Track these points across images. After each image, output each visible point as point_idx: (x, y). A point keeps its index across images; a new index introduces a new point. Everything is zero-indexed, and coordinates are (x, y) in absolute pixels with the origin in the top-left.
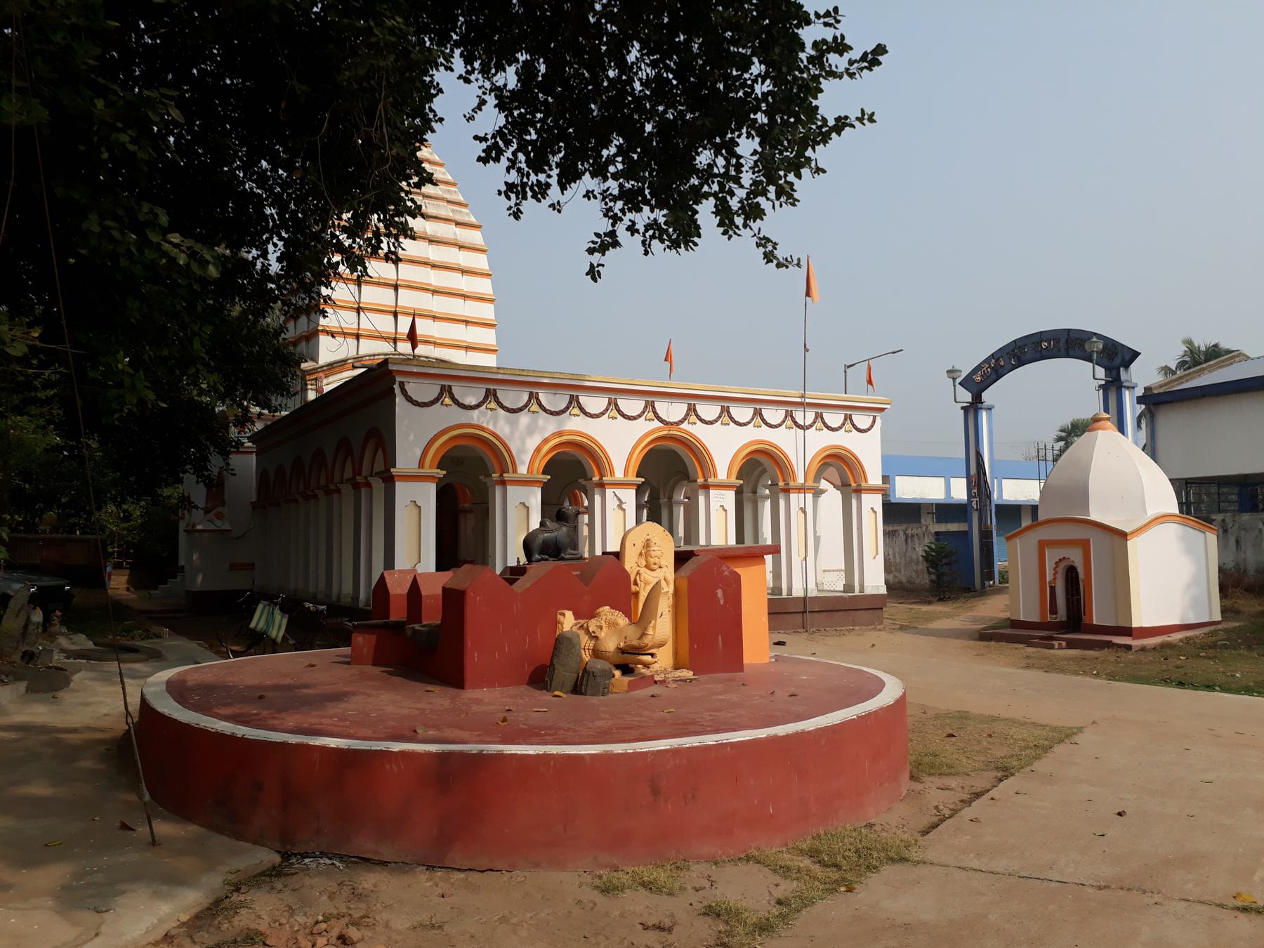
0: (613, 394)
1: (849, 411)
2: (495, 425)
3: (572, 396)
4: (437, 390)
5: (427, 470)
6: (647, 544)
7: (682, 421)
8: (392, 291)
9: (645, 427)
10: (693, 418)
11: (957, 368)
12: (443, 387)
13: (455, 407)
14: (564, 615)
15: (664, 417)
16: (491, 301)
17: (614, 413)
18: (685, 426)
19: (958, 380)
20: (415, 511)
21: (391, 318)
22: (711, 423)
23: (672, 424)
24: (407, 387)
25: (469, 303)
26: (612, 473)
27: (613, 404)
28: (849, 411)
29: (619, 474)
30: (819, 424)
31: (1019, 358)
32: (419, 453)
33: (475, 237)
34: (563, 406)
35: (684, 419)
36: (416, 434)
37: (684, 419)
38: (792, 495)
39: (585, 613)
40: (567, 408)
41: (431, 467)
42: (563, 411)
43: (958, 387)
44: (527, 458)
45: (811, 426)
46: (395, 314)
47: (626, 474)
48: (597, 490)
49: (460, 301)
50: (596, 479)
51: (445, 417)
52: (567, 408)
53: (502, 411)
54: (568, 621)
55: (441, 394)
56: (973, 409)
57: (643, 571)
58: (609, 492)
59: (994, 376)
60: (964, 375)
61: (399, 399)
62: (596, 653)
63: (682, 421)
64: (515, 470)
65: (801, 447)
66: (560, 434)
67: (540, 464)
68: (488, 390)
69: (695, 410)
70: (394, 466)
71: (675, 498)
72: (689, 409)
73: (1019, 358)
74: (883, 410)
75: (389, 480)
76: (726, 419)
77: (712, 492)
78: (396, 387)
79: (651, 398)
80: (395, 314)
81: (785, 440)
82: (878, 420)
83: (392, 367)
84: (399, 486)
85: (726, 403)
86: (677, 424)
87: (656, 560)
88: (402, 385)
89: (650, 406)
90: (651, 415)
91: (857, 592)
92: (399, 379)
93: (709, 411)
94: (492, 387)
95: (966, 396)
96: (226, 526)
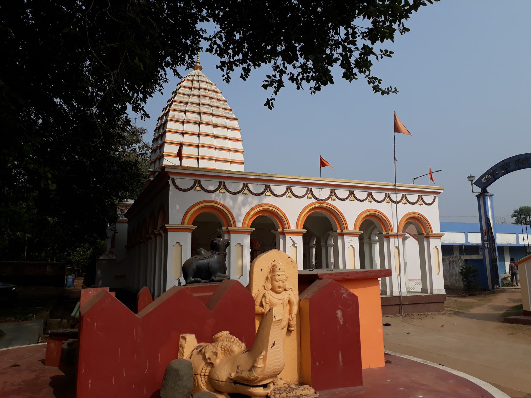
0: (289, 184)
1: (420, 193)
3: (266, 186)
4: (192, 183)
5: (186, 225)
6: (273, 270)
7: (327, 199)
8: (196, 149)
10: (334, 197)
11: (472, 175)
12: (196, 181)
13: (202, 191)
14: (185, 338)
15: (318, 197)
16: (242, 152)
17: (290, 195)
18: (329, 201)
19: (474, 182)
20: (180, 248)
21: (196, 161)
22: (344, 200)
23: (322, 200)
24: (176, 181)
25: (232, 153)
26: (289, 227)
27: (289, 190)
28: (420, 193)
29: (293, 228)
30: (404, 201)
31: (506, 169)
33: (235, 124)
34: (262, 190)
36: (180, 206)
38: (390, 239)
39: (206, 337)
40: (264, 192)
41: (188, 224)
42: (262, 194)
43: (474, 185)
44: (242, 219)
45: (400, 202)
46: (198, 159)
47: (297, 227)
48: (281, 236)
49: (228, 152)
50: (280, 230)
52: (264, 192)
53: (228, 194)
54: (190, 343)
55: (195, 184)
56: (482, 196)
57: (270, 294)
58: (287, 237)
59: (493, 179)
60: (476, 179)
61: (172, 187)
62: (211, 381)
63: (327, 199)
64: (235, 225)
65: (395, 213)
66: (260, 205)
67: (249, 222)
68: (220, 183)
69: (335, 193)
70: (168, 224)
71: (329, 242)
72: (331, 192)
73: (506, 169)
74: (439, 193)
75: (166, 231)
76: (352, 198)
77: (346, 238)
78: (170, 181)
79: (310, 186)
80: (198, 159)
81: (386, 209)
82: (437, 199)
83: (167, 170)
84: (170, 234)
85: (352, 189)
87: (281, 284)
88: (173, 180)
89: (309, 191)
90: (310, 196)
91: (429, 293)
92: (171, 176)
93: (343, 193)
94: (223, 181)
95: (478, 190)
96: (114, 257)
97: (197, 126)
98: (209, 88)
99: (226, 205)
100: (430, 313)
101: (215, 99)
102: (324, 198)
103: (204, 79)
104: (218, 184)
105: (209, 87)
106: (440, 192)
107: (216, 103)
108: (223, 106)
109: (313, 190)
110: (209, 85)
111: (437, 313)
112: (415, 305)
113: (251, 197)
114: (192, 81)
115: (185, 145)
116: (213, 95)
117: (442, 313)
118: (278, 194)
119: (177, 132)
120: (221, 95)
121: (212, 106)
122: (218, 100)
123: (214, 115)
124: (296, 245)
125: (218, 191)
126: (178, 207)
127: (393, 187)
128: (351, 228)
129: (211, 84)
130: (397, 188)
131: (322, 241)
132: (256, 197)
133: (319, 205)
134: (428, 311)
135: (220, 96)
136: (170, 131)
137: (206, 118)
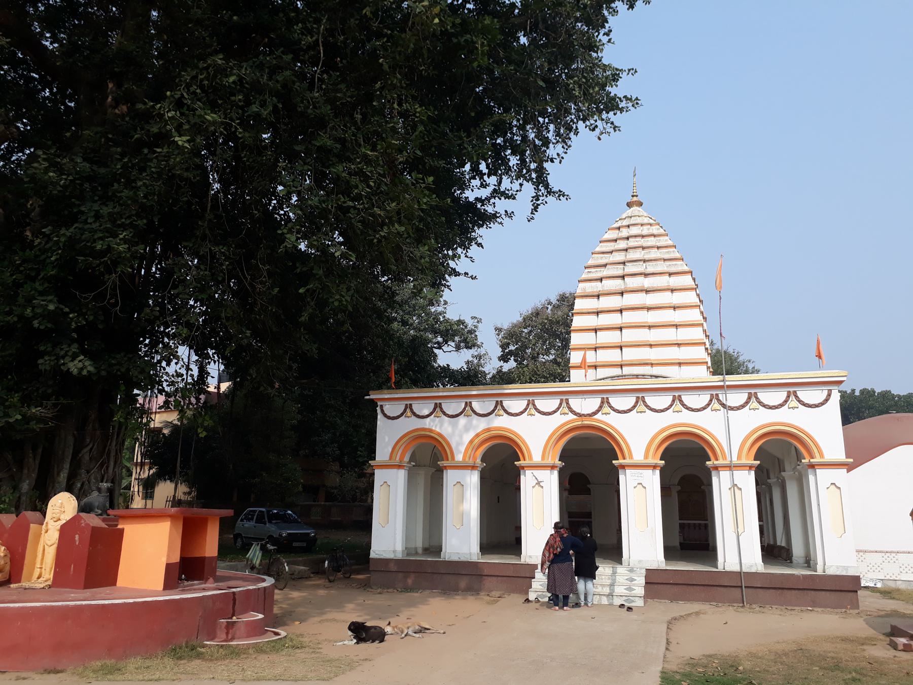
2: (441, 428)
4: (403, 407)
7: (595, 413)
10: (606, 409)
15: (578, 411)
17: (533, 411)
18: (599, 416)
24: (385, 409)
26: (531, 458)
28: (792, 388)
29: (537, 457)
32: (390, 450)
44: (463, 449)
46: (621, 348)
51: (409, 424)
52: (493, 411)
55: (405, 410)
61: (380, 416)
63: (595, 413)
69: (608, 403)
70: (374, 459)
78: (378, 409)
80: (621, 348)
81: (710, 424)
85: (640, 395)
86: (590, 415)
88: (381, 406)
90: (566, 410)
91: (820, 571)
94: (438, 402)
97: (619, 297)
98: (645, 232)
99: (443, 433)
100: (819, 610)
101: (652, 247)
102: (590, 412)
103: (639, 220)
104: (432, 406)
105: (645, 230)
106: (841, 382)
107: (654, 254)
108: (667, 256)
109: (571, 401)
110: (645, 227)
111: (839, 610)
114: (619, 228)
115: (601, 329)
116: (651, 241)
117: (851, 611)
118: (513, 412)
119: (589, 313)
120: (666, 238)
121: (645, 261)
122: (658, 248)
123: (646, 275)
126: (387, 439)
127: (722, 384)
129: (651, 225)
130: (727, 383)
131: (772, 476)
134: (814, 604)
135: (664, 241)
136: (578, 313)
137: (631, 282)
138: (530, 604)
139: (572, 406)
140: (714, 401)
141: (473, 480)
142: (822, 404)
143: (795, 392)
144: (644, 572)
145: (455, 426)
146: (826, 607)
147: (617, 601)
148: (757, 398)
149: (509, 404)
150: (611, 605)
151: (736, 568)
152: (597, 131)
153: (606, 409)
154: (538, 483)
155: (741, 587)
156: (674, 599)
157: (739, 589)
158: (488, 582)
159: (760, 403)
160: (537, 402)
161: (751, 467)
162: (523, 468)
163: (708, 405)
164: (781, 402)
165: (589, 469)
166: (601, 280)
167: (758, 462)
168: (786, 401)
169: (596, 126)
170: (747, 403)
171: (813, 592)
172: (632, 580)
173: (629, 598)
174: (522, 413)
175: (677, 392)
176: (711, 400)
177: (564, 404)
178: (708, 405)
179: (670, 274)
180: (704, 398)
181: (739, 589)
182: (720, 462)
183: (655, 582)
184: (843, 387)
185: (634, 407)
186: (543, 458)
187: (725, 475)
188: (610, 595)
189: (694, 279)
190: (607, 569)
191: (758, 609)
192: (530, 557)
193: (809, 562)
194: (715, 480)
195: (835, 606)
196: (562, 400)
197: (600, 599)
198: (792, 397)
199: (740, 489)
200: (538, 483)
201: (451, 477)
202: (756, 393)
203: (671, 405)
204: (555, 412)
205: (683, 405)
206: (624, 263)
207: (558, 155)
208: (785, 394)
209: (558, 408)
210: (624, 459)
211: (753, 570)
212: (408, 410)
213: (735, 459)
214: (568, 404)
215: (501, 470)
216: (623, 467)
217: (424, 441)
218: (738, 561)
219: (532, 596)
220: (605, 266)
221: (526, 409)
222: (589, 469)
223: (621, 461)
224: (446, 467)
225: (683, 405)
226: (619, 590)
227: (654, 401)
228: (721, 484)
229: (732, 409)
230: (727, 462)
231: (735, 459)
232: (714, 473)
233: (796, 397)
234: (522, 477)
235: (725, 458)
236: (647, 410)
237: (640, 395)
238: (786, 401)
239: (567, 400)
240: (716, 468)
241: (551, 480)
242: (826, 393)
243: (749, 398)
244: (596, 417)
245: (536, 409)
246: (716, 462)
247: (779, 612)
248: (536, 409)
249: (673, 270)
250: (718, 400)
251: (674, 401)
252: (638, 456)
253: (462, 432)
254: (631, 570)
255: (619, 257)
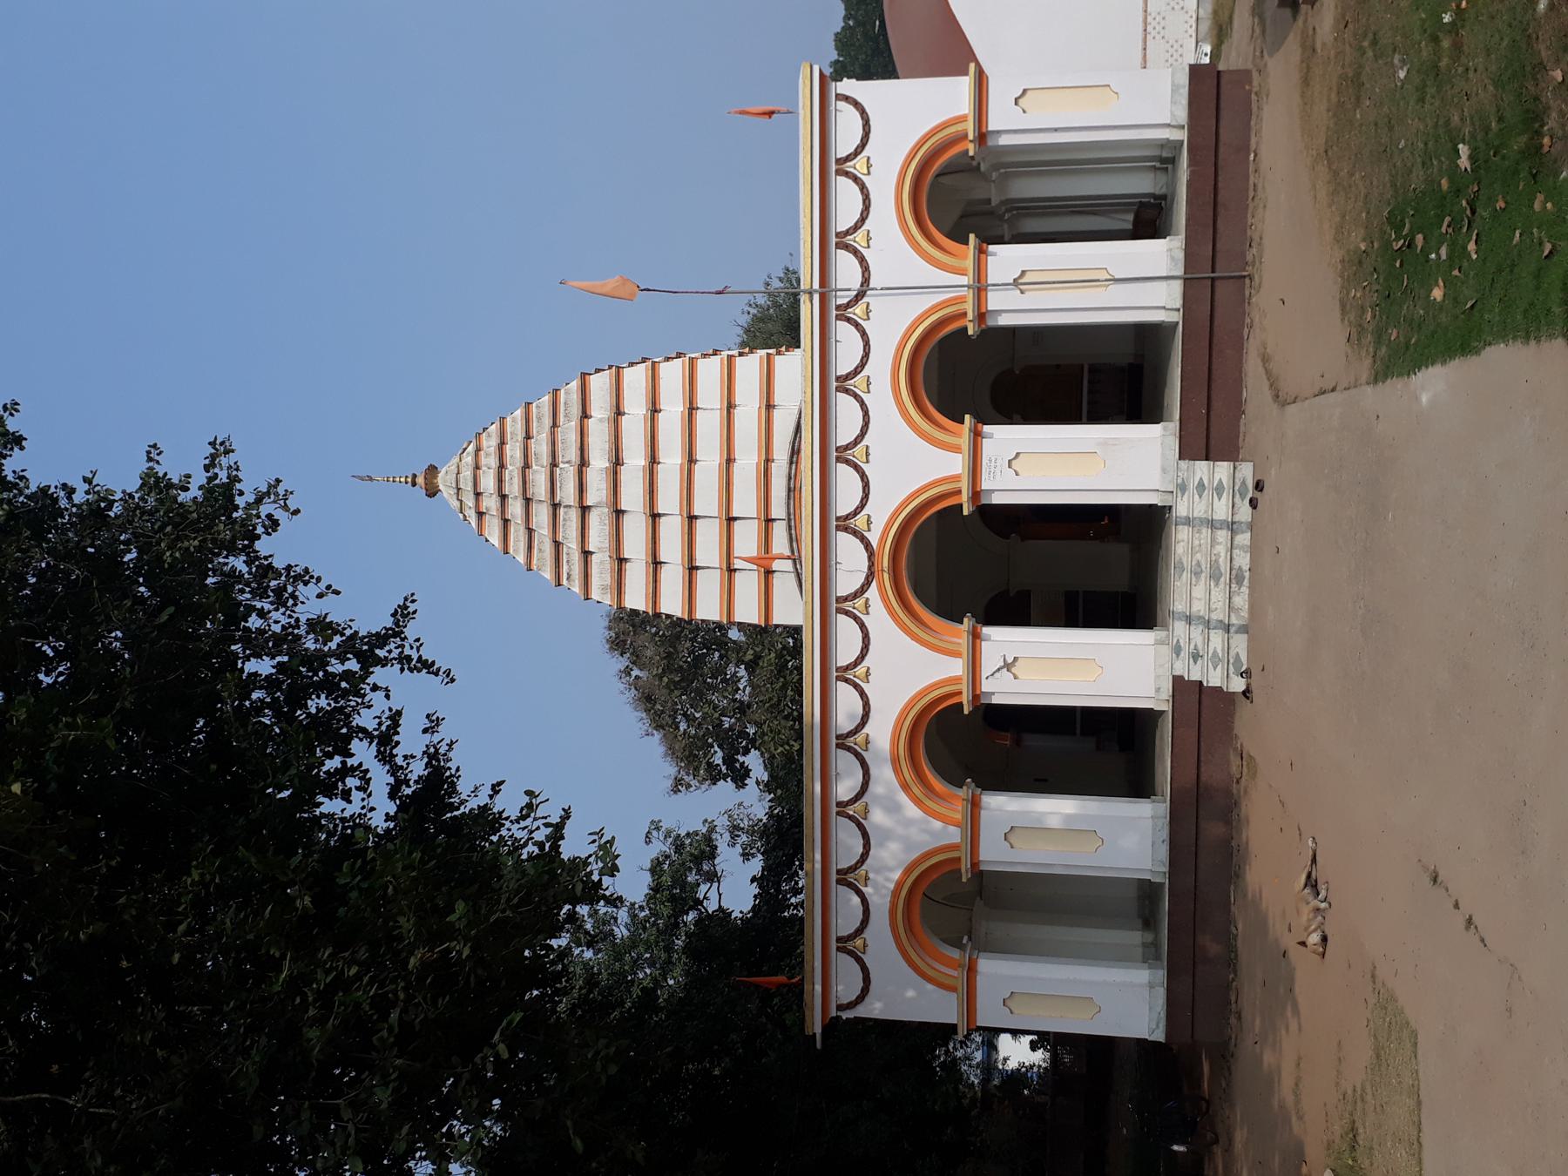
1: (830, 167)
2: (891, 870)
9: (879, 617)
10: (859, 522)
17: (860, 670)
18: (874, 538)
23: (870, 568)
26: (957, 680)
27: (844, 674)
28: (830, 167)
29: (956, 668)
32: (930, 987)
35: (863, 539)
37: (863, 539)
51: (880, 942)
65: (905, 284)
69: (847, 517)
81: (893, 324)
90: (860, 602)
91: (1182, 135)
94: (834, 877)
106: (822, 75)
109: (842, 592)
112: (1221, 210)
113: (876, 788)
124: (1010, 660)
125: (864, 889)
127: (816, 297)
128: (955, 464)
130: (816, 286)
132: (873, 771)
133: (886, 576)
138: (1254, 687)
139: (852, 590)
140: (850, 313)
141: (1001, 806)
142: (863, 112)
143: (839, 161)
144: (1184, 464)
145: (887, 835)
146: (1248, 127)
147: (1245, 513)
148: (847, 233)
149: (844, 720)
150: (1251, 526)
151: (1177, 287)
152: (279, 515)
153: (859, 522)
154: (1008, 666)
155: (1213, 279)
156: (1237, 408)
157: (1218, 283)
158: (1211, 774)
159: (856, 227)
160: (842, 662)
161: (981, 251)
162: (976, 697)
163: (857, 325)
164: (856, 189)
165: (980, 563)
166: (586, 554)
167: (972, 237)
168: (856, 179)
169: (269, 516)
170: (856, 252)
171: (1222, 150)
172: (1201, 487)
173: (1237, 490)
174: (862, 694)
175: (831, 384)
176: (849, 320)
177: (848, 606)
178: (857, 325)
179: (585, 415)
180: (843, 331)
181: (1215, 280)
182: (969, 308)
183: (1206, 439)
184: (828, 71)
185: (856, 467)
186: (955, 654)
187: (994, 301)
188: (1232, 527)
189: (598, 371)
190: (1180, 537)
191: (1254, 250)
192: (1158, 690)
193: (1164, 159)
194: (1004, 321)
195: (1246, 112)
196: (839, 611)
197: (1242, 548)
198: (848, 167)
199: (1023, 272)
200: (1008, 666)
201: (994, 854)
202: (838, 235)
203: (856, 396)
204: (862, 626)
205: (856, 372)
206: (555, 507)
207: (320, 596)
208: (842, 180)
209: (856, 618)
210: (959, 492)
211: (1181, 255)
212: (850, 945)
213: (964, 280)
214: (846, 599)
215: (979, 744)
216: (976, 494)
217: (917, 909)
218: (1164, 284)
219: (1238, 685)
220: (557, 545)
221: (856, 686)
222: (980, 563)
223: (964, 498)
224: (975, 864)
225: (856, 372)
226: (1221, 510)
227: (845, 431)
228: (1013, 308)
229: (866, 280)
230: (970, 295)
231: (964, 280)
232: (990, 322)
233: (848, 158)
234: (996, 700)
235: (962, 300)
236: (864, 443)
237: (833, 455)
238: (856, 179)
239: (839, 600)
240: (981, 316)
241: (1001, 640)
242: (842, 105)
243: (847, 247)
244: (875, 544)
245: (856, 663)
246: (970, 316)
247: (1260, 210)
248: (856, 663)
249: (575, 410)
250: (848, 305)
251: (847, 391)
252: (955, 464)
253: (900, 826)
254: (1183, 488)
255: (541, 516)
